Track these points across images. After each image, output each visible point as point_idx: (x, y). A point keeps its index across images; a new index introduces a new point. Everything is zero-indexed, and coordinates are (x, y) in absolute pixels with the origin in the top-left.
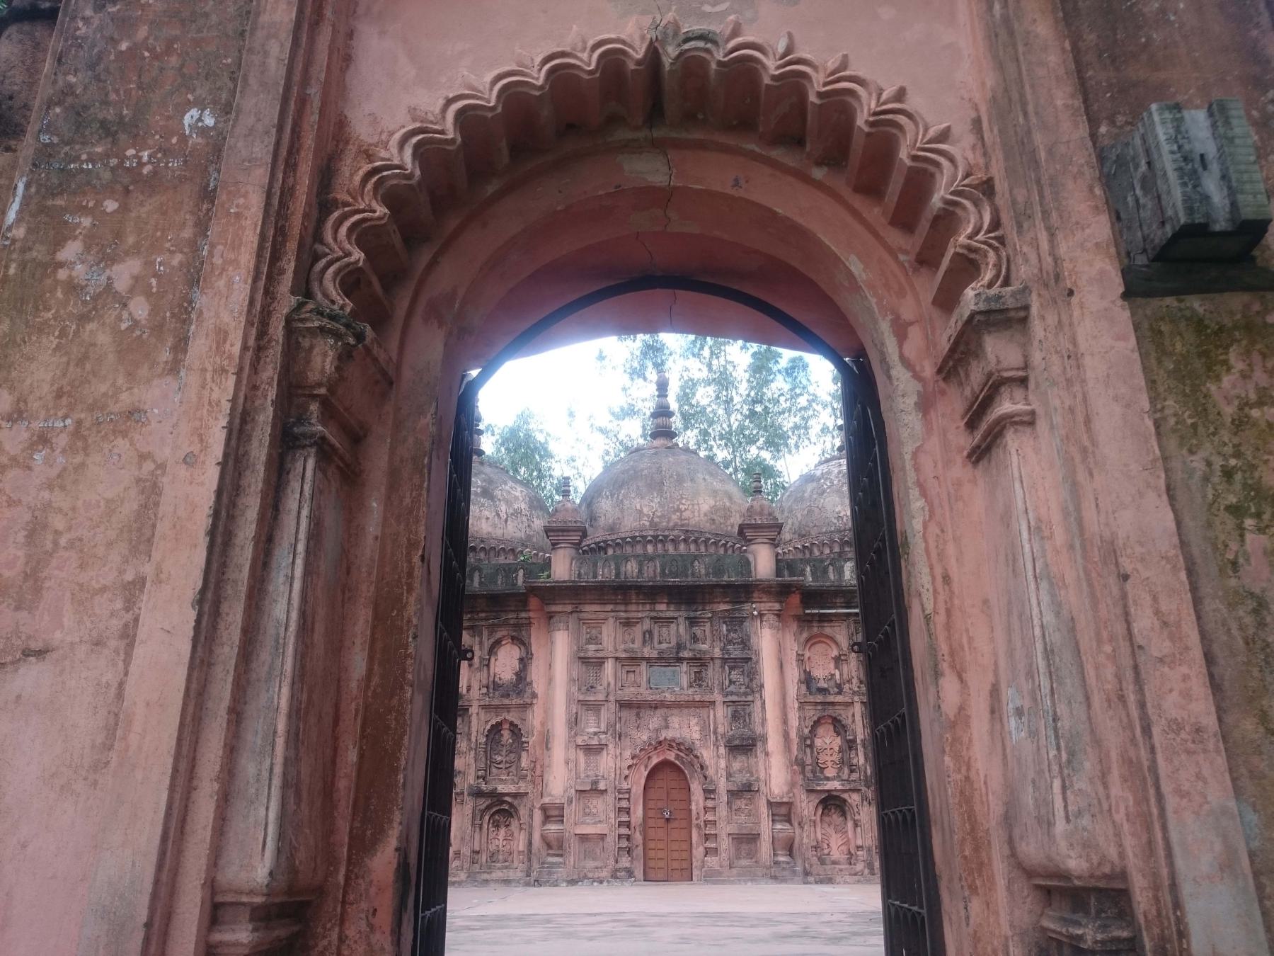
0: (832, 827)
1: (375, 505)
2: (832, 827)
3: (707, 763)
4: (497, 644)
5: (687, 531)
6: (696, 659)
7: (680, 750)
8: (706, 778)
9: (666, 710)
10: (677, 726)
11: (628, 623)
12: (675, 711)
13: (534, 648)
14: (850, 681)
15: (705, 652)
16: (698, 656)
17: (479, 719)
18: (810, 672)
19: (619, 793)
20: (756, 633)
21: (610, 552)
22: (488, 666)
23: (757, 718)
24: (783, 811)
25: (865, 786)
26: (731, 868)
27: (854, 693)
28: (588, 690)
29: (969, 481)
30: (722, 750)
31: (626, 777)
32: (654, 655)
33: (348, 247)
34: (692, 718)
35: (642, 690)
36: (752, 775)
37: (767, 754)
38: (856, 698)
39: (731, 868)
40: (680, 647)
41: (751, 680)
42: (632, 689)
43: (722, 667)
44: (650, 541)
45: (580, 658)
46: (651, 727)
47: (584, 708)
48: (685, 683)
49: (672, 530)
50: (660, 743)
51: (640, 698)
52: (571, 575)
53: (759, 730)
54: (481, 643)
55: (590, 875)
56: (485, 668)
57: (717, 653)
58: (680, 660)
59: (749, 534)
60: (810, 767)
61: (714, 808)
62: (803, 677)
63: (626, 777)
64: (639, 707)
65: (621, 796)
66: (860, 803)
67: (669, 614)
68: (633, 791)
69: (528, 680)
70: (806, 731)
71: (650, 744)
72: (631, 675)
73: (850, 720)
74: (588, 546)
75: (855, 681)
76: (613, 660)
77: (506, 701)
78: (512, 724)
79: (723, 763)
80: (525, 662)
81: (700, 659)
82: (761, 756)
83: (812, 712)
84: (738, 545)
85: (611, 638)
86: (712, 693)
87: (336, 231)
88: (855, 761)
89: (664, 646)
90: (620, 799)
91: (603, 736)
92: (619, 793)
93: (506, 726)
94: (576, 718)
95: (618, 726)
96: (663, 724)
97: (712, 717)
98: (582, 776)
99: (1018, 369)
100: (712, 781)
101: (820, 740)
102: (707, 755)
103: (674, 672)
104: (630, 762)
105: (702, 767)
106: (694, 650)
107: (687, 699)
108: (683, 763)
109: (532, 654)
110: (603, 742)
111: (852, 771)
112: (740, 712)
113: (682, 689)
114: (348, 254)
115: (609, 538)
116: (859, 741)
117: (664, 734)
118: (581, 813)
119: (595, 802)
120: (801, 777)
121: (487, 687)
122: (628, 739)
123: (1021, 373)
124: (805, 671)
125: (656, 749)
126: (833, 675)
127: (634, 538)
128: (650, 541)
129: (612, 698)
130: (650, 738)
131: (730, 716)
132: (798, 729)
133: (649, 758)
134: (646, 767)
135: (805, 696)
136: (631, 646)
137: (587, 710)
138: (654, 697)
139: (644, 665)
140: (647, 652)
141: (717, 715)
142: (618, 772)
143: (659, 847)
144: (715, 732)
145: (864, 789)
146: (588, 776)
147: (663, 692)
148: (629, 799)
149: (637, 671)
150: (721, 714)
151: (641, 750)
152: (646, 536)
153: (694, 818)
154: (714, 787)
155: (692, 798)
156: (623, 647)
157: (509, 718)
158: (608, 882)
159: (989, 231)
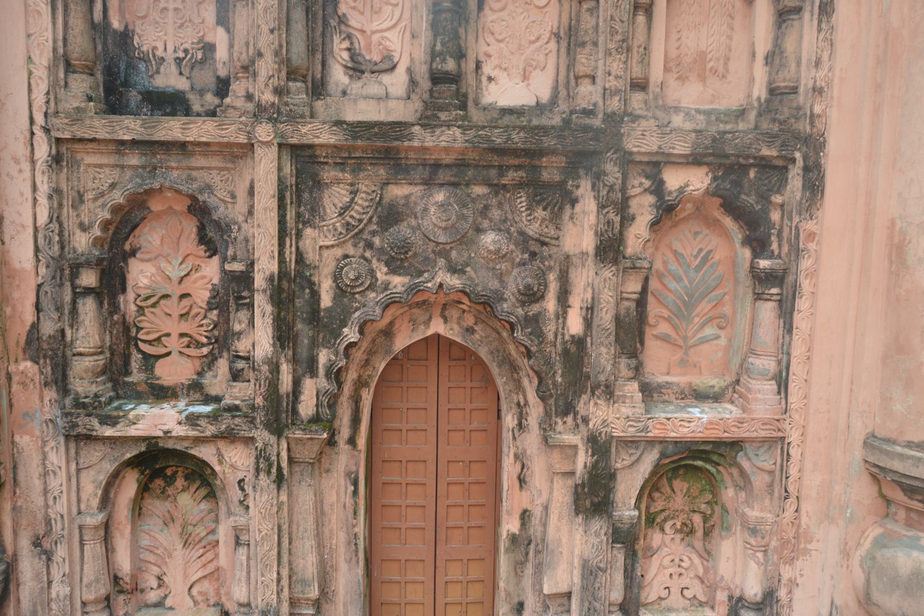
0: (176, 529)
2: (176, 529)
14: (248, 69)
18: (125, 37)
25: (267, 426)
27: (260, 112)
38: (264, 132)
60: (88, 362)
66: (250, 478)
73: (241, 206)
75: (266, 67)
83: (108, 177)
88: (242, 346)
101: (149, 269)
111: (236, 376)
116: (259, 281)
120: (51, 394)
126: (209, 48)
135: (77, 116)
145: (262, 436)
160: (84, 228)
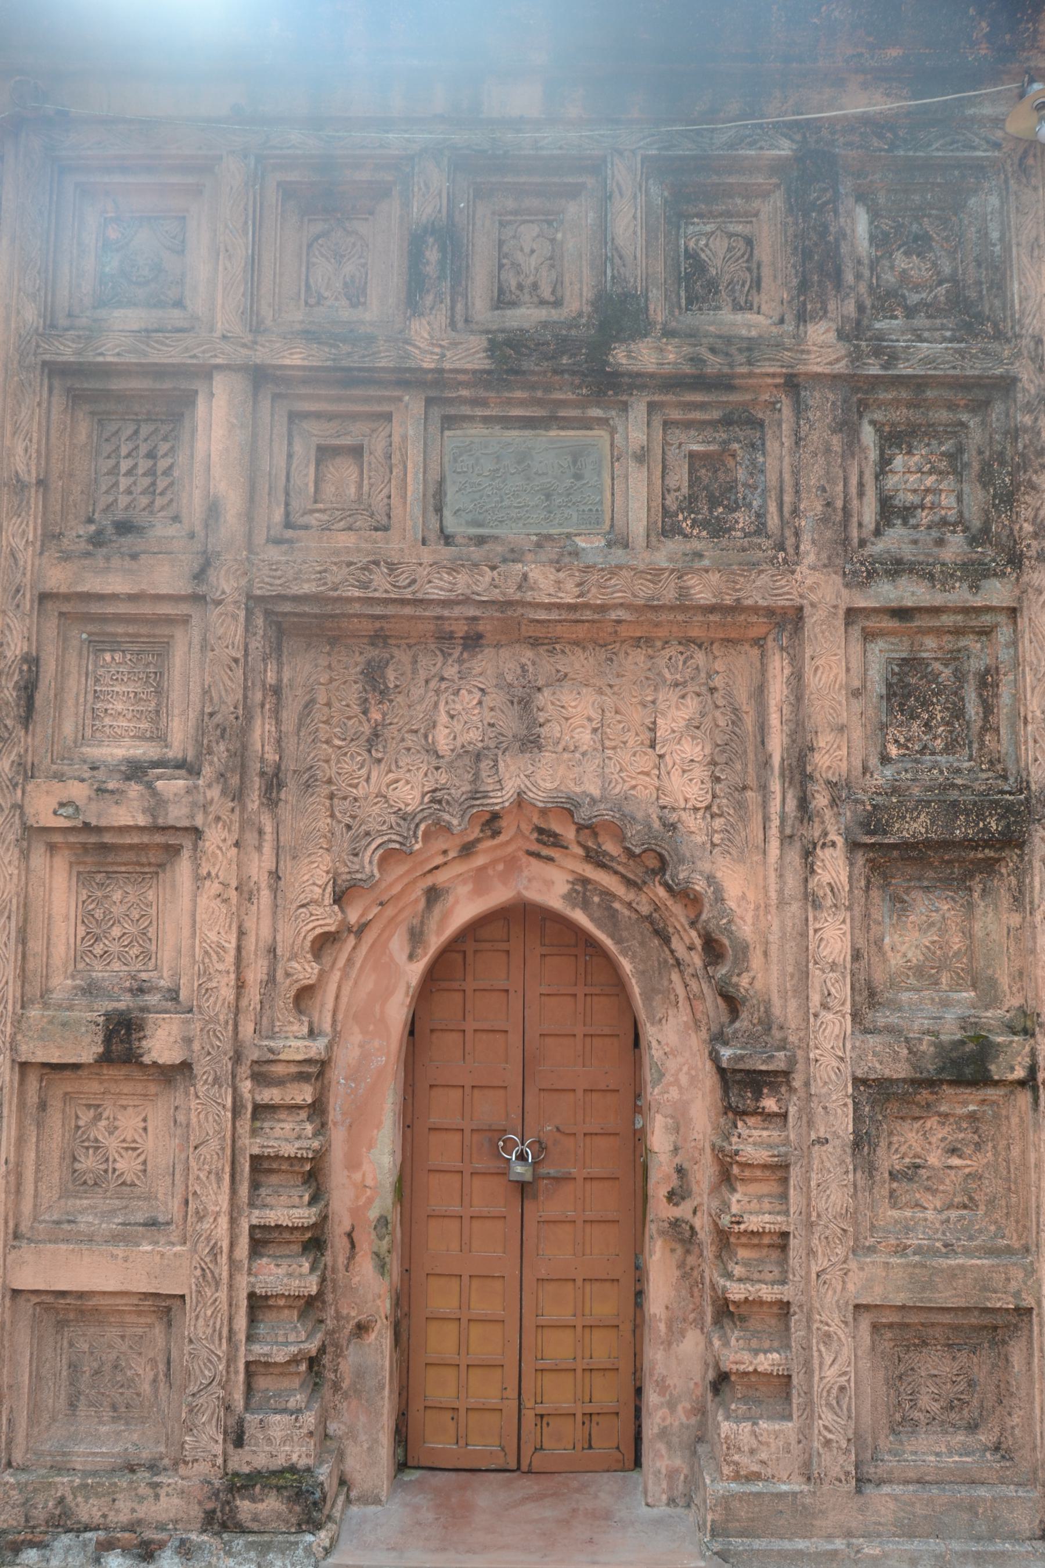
3: (746, 930)
6: (700, 382)
7: (595, 858)
8: (732, 1003)
9: (527, 655)
10: (585, 738)
15: (751, 347)
16: (714, 364)
19: (260, 1078)
26: (861, 1481)
28: (97, 540)
31: (304, 995)
34: (667, 697)
35: (393, 546)
36: (989, 994)
39: (861, 1481)
41: (1007, 499)
42: (346, 540)
43: (848, 428)
45: (55, 370)
46: (442, 739)
47: (79, 635)
48: (638, 524)
50: (492, 822)
51: (381, 584)
55: (87, 1510)
61: (779, 1170)
63: (304, 995)
64: (379, 638)
65: (270, 1095)
68: (347, 1056)
72: (344, 472)
81: (724, 383)
86: (789, 566)
90: (261, 1111)
91: (172, 786)
92: (260, 1078)
94: (28, 690)
95: (261, 730)
96: (510, 724)
97: (777, 691)
98: (62, 984)
100: (767, 1024)
103: (577, 456)
104: (328, 919)
106: (692, 335)
107: (644, 591)
108: (610, 919)
110: (176, 815)
113: (619, 541)
118: (54, 1176)
119: (129, 1123)
122: (317, 802)
125: (467, 850)
130: (436, 798)
131: (878, 687)
133: (433, 895)
134: (416, 937)
136: (346, 314)
137: (98, 645)
138: (463, 582)
141: (814, 681)
142: (256, 973)
143: (479, 1307)
146: (91, 990)
147: (515, 555)
148: (317, 1109)
149: (379, 446)
151: (387, 858)
153: (659, 1186)
154: (780, 1061)
155: (654, 1093)
156: (296, 316)
158: (185, 1550)
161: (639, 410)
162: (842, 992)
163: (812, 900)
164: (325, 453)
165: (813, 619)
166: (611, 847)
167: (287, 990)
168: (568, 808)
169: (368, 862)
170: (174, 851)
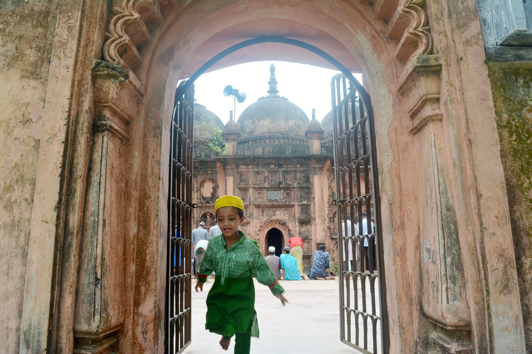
1: (137, 154)
4: (204, 181)
5: (283, 134)
7: (280, 224)
11: (258, 173)
12: (278, 209)
13: (219, 184)
15: (290, 185)
17: (197, 212)
20: (312, 177)
21: (250, 143)
22: (200, 190)
23: (312, 210)
24: (321, 247)
29: (411, 143)
30: (297, 224)
31: (258, 234)
32: (269, 186)
33: (121, 33)
37: (315, 225)
40: (280, 183)
42: (260, 200)
44: (267, 138)
45: (238, 188)
49: (277, 133)
50: (272, 221)
52: (233, 153)
53: (313, 216)
54: (196, 181)
56: (199, 191)
57: (296, 185)
58: (280, 189)
59: (310, 135)
62: (331, 194)
63: (258, 234)
67: (275, 170)
68: (261, 240)
69: (217, 196)
70: (331, 215)
71: (268, 222)
72: (260, 194)
74: (241, 140)
76: (252, 188)
77: (208, 205)
78: (211, 213)
79: (297, 229)
80: (215, 189)
82: (313, 227)
84: (305, 140)
85: (252, 180)
87: (115, 26)
89: (273, 183)
93: (208, 214)
96: (273, 214)
99: (436, 94)
102: (291, 225)
104: (260, 229)
105: (289, 230)
109: (218, 186)
112: (306, 209)
114: (121, 37)
115: (250, 137)
117: (274, 218)
121: (200, 199)
123: (437, 96)
124: (332, 192)
127: (260, 137)
128: (267, 138)
129: (252, 204)
132: (328, 215)
139: (265, 191)
140: (266, 185)
144: (295, 217)
149: (262, 192)
150: (297, 210)
152: (266, 136)
157: (209, 211)
159: (424, 26)
160: (332, 214)
161: (282, 190)
162: (298, 232)
163: (296, 226)
164: (258, 193)
165: (295, 206)
166: (281, 223)
167: (257, 234)
168: (278, 220)
169: (262, 225)
170: (248, 224)
